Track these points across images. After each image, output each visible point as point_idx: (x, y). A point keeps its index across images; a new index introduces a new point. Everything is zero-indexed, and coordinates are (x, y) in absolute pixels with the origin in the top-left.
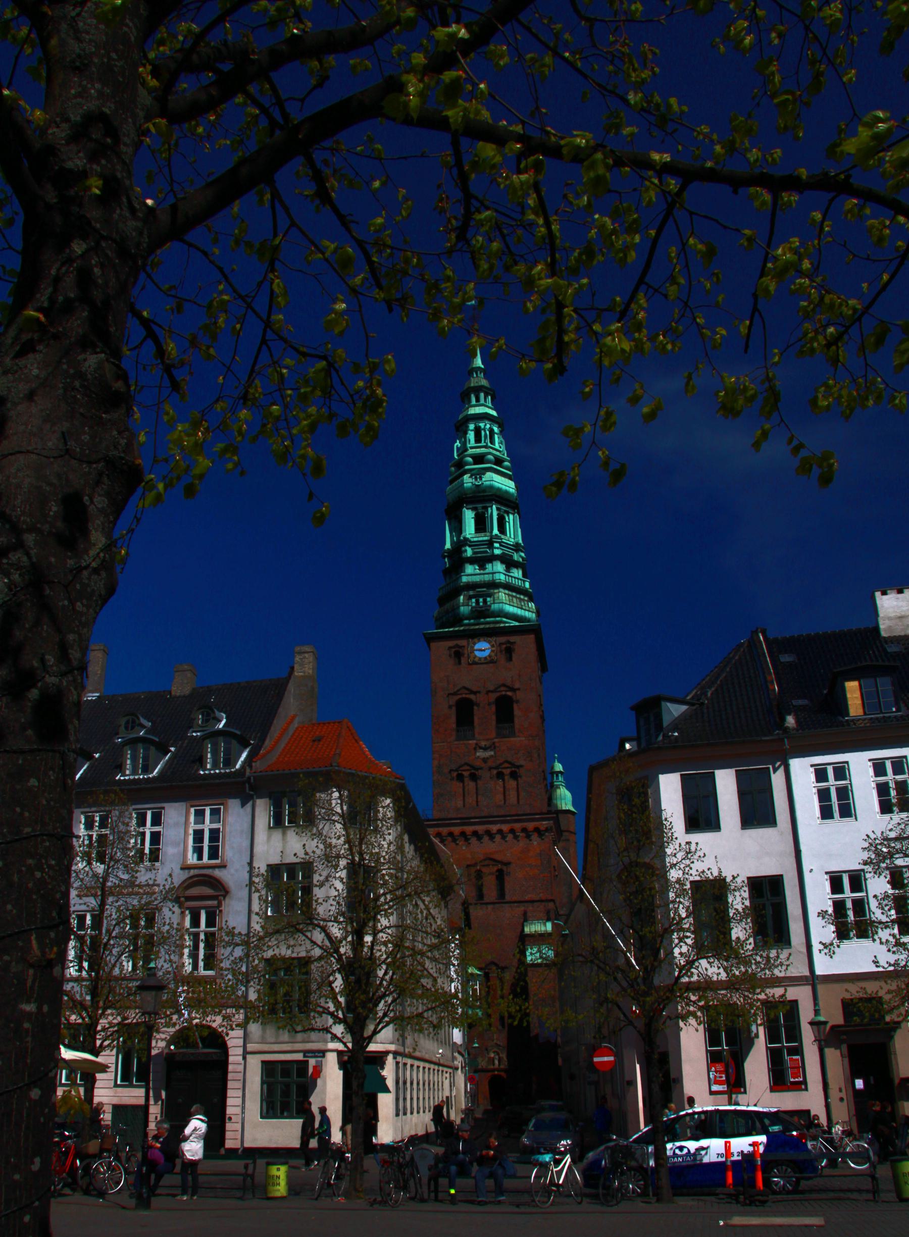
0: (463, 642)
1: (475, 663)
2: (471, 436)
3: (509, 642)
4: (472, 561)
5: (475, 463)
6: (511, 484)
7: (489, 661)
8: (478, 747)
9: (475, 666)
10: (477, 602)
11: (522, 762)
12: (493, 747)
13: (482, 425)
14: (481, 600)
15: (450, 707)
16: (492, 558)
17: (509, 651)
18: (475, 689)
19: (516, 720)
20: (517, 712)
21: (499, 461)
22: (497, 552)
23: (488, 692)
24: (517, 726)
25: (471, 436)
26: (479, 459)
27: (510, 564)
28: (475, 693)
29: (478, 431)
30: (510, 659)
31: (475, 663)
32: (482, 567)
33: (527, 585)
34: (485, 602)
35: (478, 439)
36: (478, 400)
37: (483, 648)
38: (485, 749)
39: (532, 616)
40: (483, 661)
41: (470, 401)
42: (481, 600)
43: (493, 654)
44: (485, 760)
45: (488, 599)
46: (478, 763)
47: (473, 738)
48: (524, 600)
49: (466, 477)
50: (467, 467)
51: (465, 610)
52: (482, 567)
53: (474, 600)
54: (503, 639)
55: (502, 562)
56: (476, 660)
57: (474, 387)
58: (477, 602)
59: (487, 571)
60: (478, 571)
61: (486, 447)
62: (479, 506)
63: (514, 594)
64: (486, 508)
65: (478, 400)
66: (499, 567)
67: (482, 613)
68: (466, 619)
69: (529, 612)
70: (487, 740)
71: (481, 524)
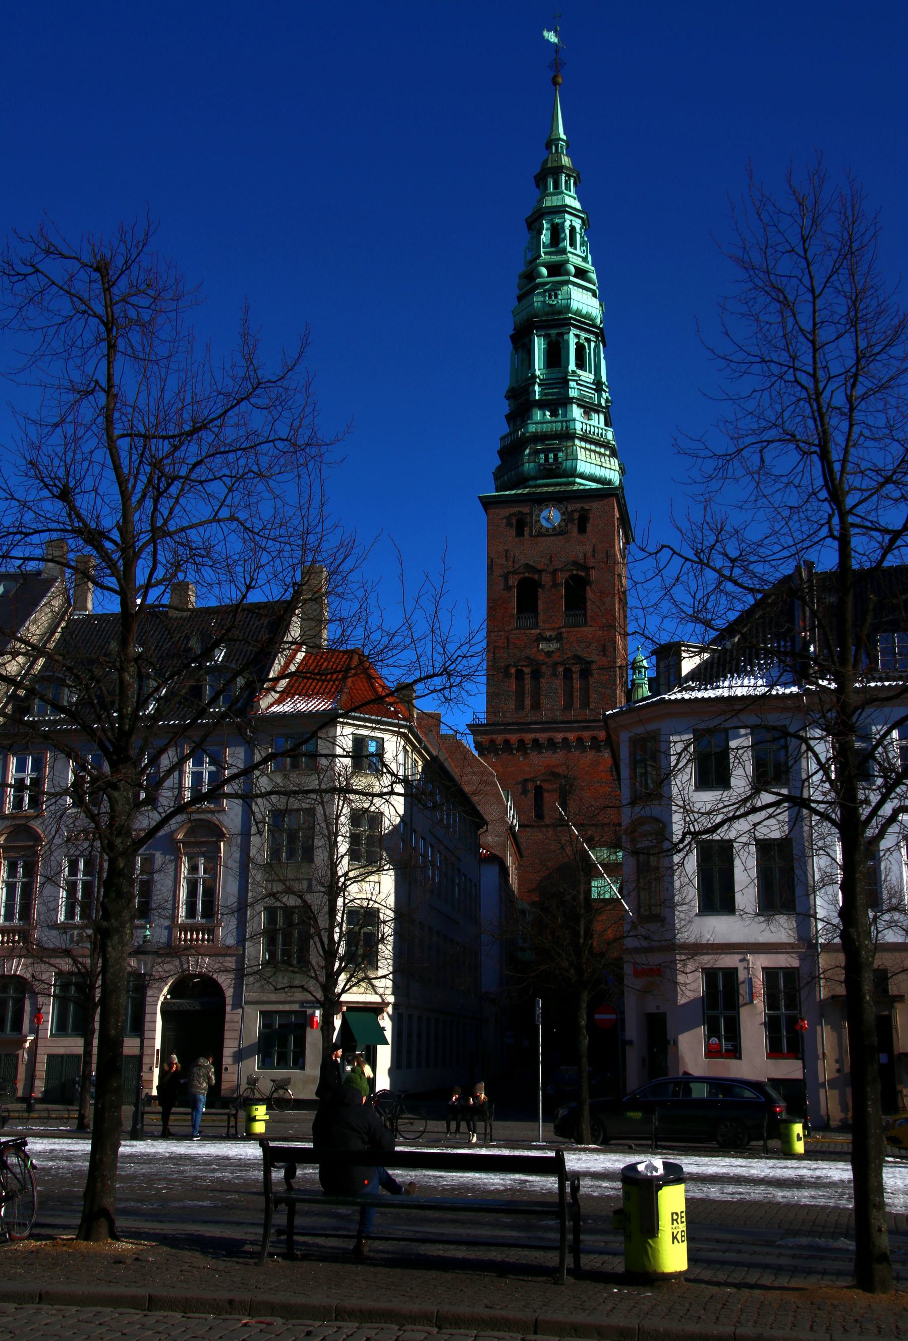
1: (540, 534)
3: (583, 509)
4: (542, 405)
6: (595, 302)
7: (558, 532)
8: (541, 638)
9: (540, 539)
10: (547, 459)
11: (594, 658)
12: (559, 638)
14: (551, 455)
15: (508, 588)
17: (583, 523)
18: (540, 567)
19: (589, 604)
20: (590, 594)
21: (581, 273)
24: (589, 613)
27: (589, 409)
28: (540, 572)
30: (582, 530)
31: (540, 534)
32: (554, 414)
33: (610, 436)
34: (556, 456)
37: (552, 516)
38: (549, 640)
39: (615, 477)
40: (550, 532)
41: (546, 187)
42: (551, 455)
43: (563, 524)
44: (549, 654)
45: (560, 454)
46: (541, 658)
47: (537, 626)
48: (604, 455)
53: (542, 456)
55: (579, 406)
56: (543, 530)
58: (547, 459)
59: (560, 418)
62: (553, 332)
63: (593, 447)
64: (561, 335)
65: (557, 186)
66: (577, 412)
69: (609, 470)
70: (553, 629)
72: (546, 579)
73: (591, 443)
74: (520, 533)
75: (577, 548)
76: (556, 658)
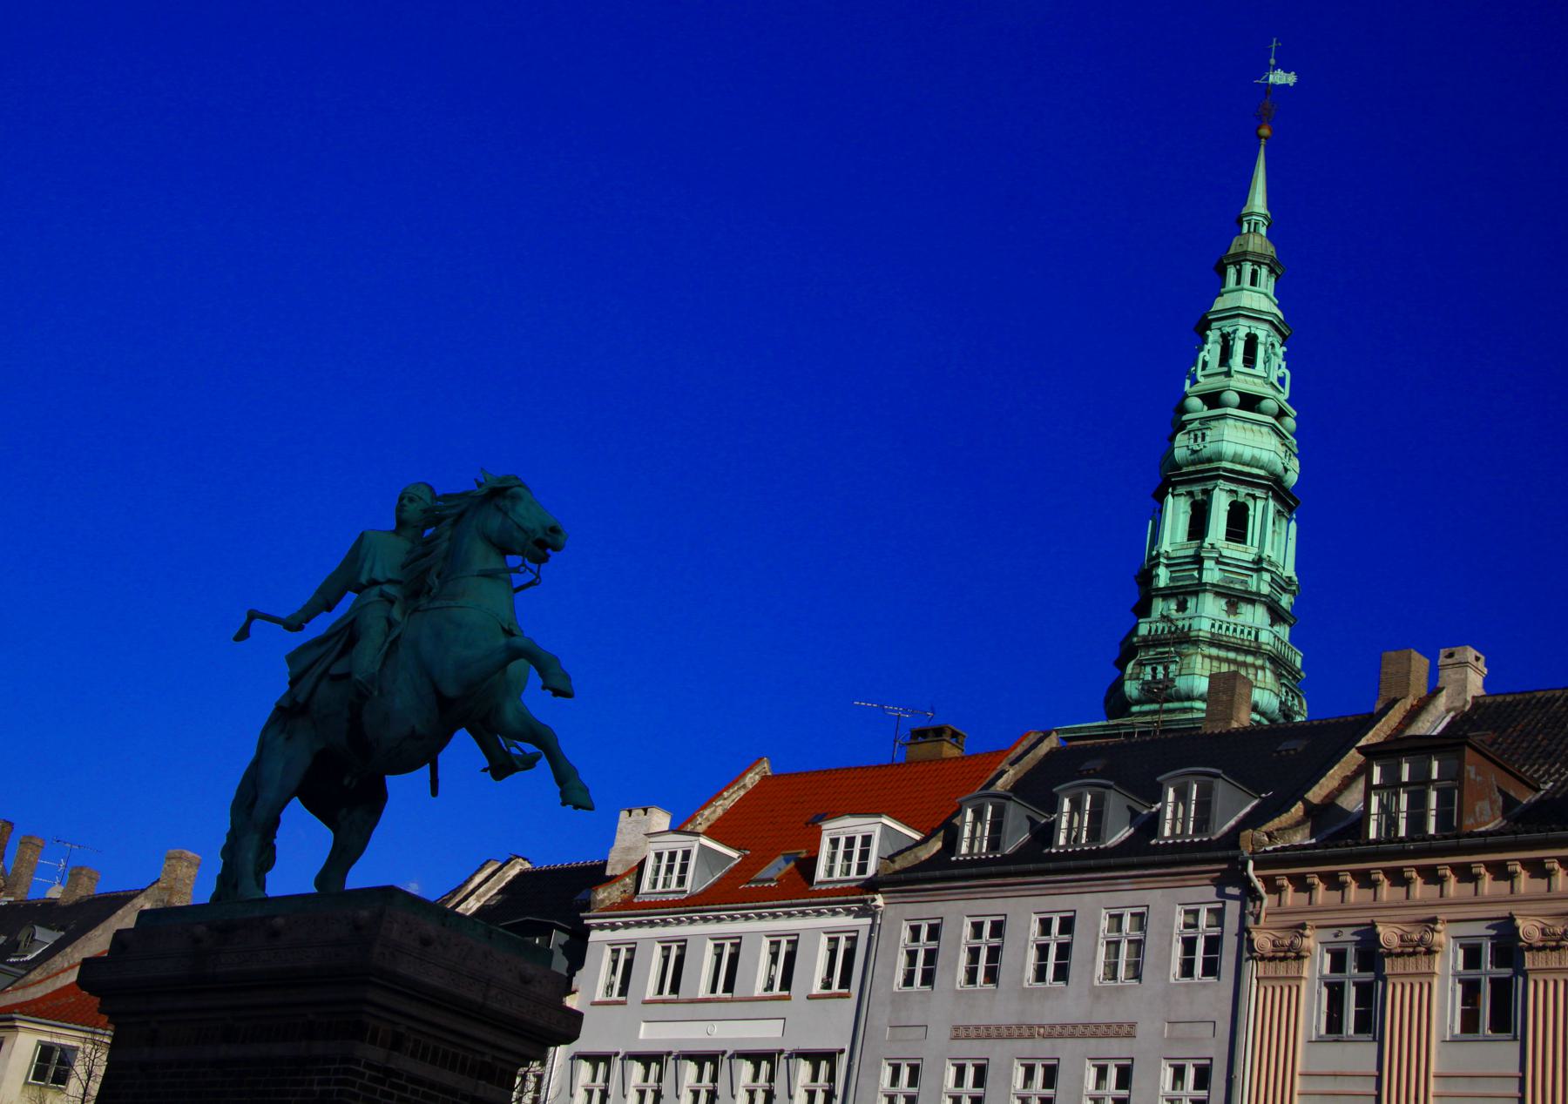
2: (1239, 348)
4: (1220, 591)
5: (1240, 407)
13: (1262, 332)
16: (1252, 598)
22: (1265, 589)
25: (1239, 348)
26: (1250, 402)
27: (1276, 615)
29: (1251, 341)
32: (1232, 607)
35: (1250, 360)
36: (1253, 283)
50: (1230, 411)
52: (1232, 607)
57: (1253, 253)
60: (1224, 616)
62: (1242, 490)
71: (1237, 527)
73: (1228, 648)
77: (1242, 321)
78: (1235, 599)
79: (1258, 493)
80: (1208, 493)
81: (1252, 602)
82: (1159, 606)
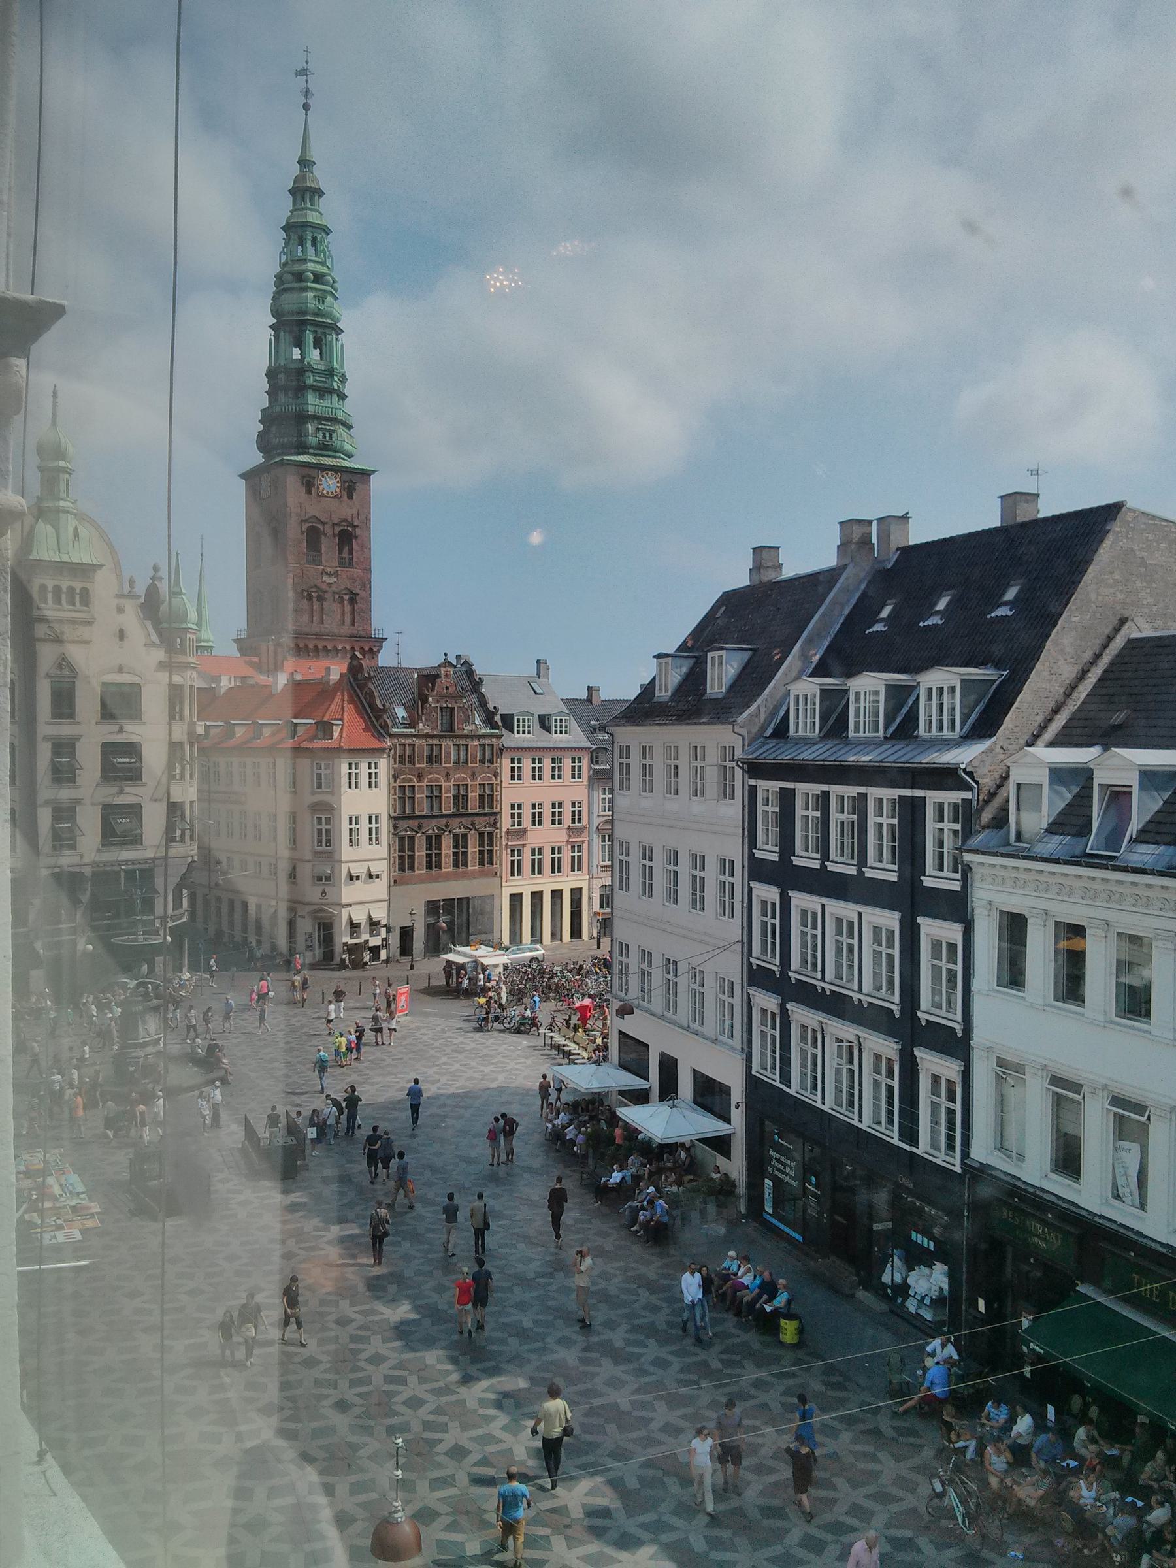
0: (313, 472)
2: (309, 243)
4: (315, 389)
8: (324, 572)
9: (323, 499)
10: (324, 437)
11: (358, 591)
12: (336, 574)
15: (302, 533)
16: (331, 391)
23: (334, 524)
26: (318, 278)
28: (324, 523)
30: (350, 497)
38: (330, 575)
44: (330, 584)
46: (324, 587)
47: (320, 563)
49: (310, 294)
50: (309, 284)
51: (312, 440)
54: (347, 477)
58: (324, 437)
61: (323, 264)
62: (319, 330)
66: (335, 397)
67: (326, 448)
68: (312, 448)
72: (328, 529)
74: (309, 492)
75: (345, 510)
76: (334, 588)
77: (309, 229)
78: (323, 392)
79: (327, 331)
80: (302, 331)
81: (331, 393)
82: (282, 398)
